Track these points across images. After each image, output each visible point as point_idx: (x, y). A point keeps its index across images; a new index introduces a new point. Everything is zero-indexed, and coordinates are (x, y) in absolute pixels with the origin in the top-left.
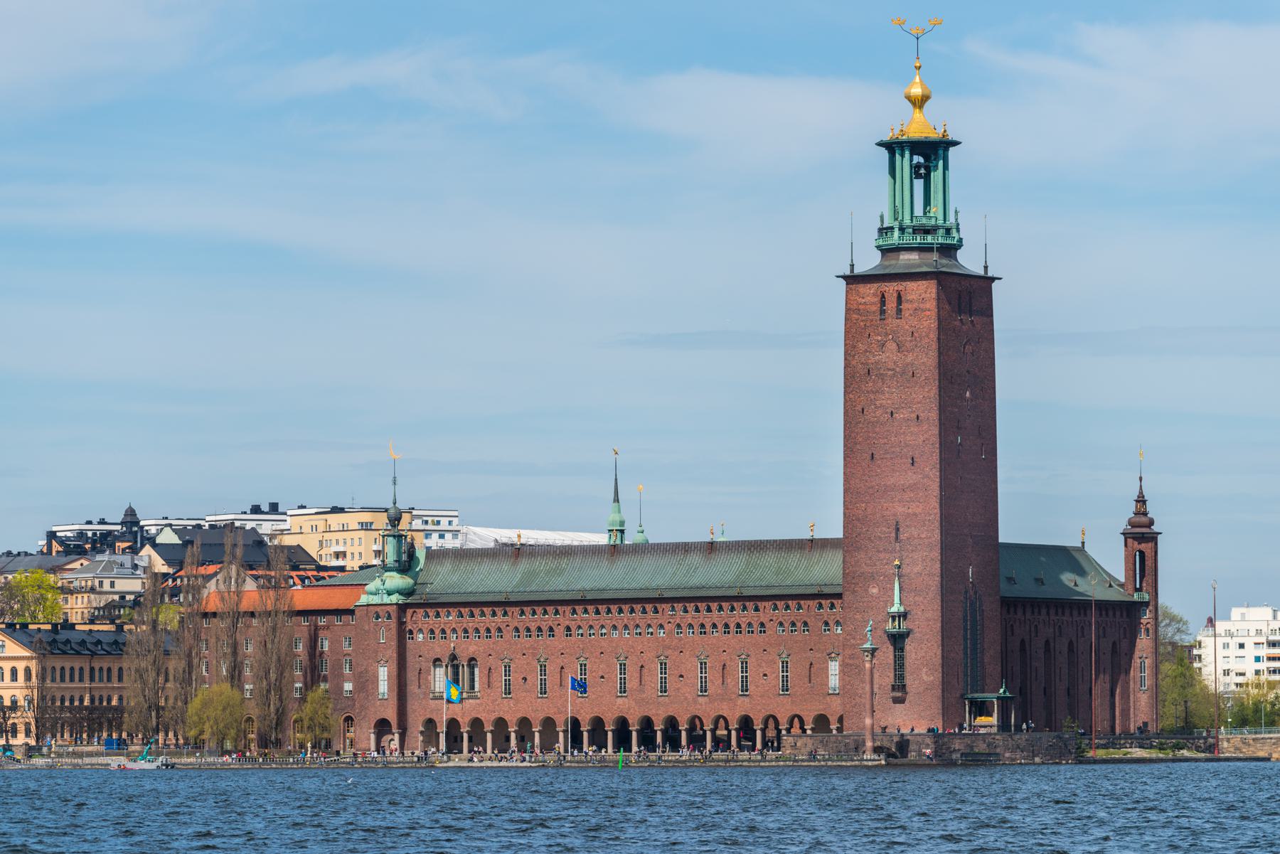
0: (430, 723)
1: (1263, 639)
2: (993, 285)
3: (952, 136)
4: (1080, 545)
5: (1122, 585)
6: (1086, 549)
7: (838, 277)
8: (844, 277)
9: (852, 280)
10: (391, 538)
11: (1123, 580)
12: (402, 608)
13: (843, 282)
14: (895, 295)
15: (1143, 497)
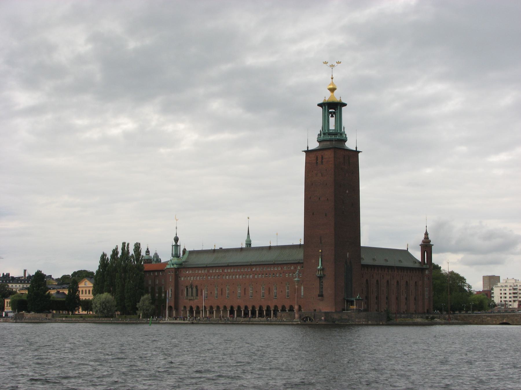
0: (185, 307)
1: (512, 288)
2: (359, 154)
3: (344, 101)
4: (407, 249)
5: (420, 263)
6: (408, 251)
7: (303, 151)
8: (305, 151)
9: (308, 152)
10: (174, 246)
11: (420, 261)
12: (176, 270)
13: (305, 154)
14: (321, 156)
15: (427, 233)
